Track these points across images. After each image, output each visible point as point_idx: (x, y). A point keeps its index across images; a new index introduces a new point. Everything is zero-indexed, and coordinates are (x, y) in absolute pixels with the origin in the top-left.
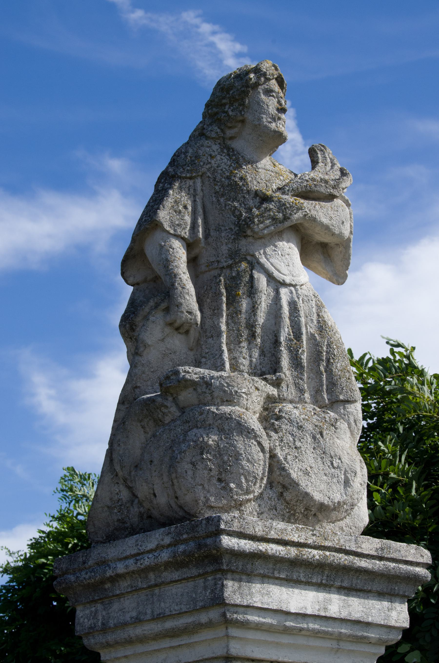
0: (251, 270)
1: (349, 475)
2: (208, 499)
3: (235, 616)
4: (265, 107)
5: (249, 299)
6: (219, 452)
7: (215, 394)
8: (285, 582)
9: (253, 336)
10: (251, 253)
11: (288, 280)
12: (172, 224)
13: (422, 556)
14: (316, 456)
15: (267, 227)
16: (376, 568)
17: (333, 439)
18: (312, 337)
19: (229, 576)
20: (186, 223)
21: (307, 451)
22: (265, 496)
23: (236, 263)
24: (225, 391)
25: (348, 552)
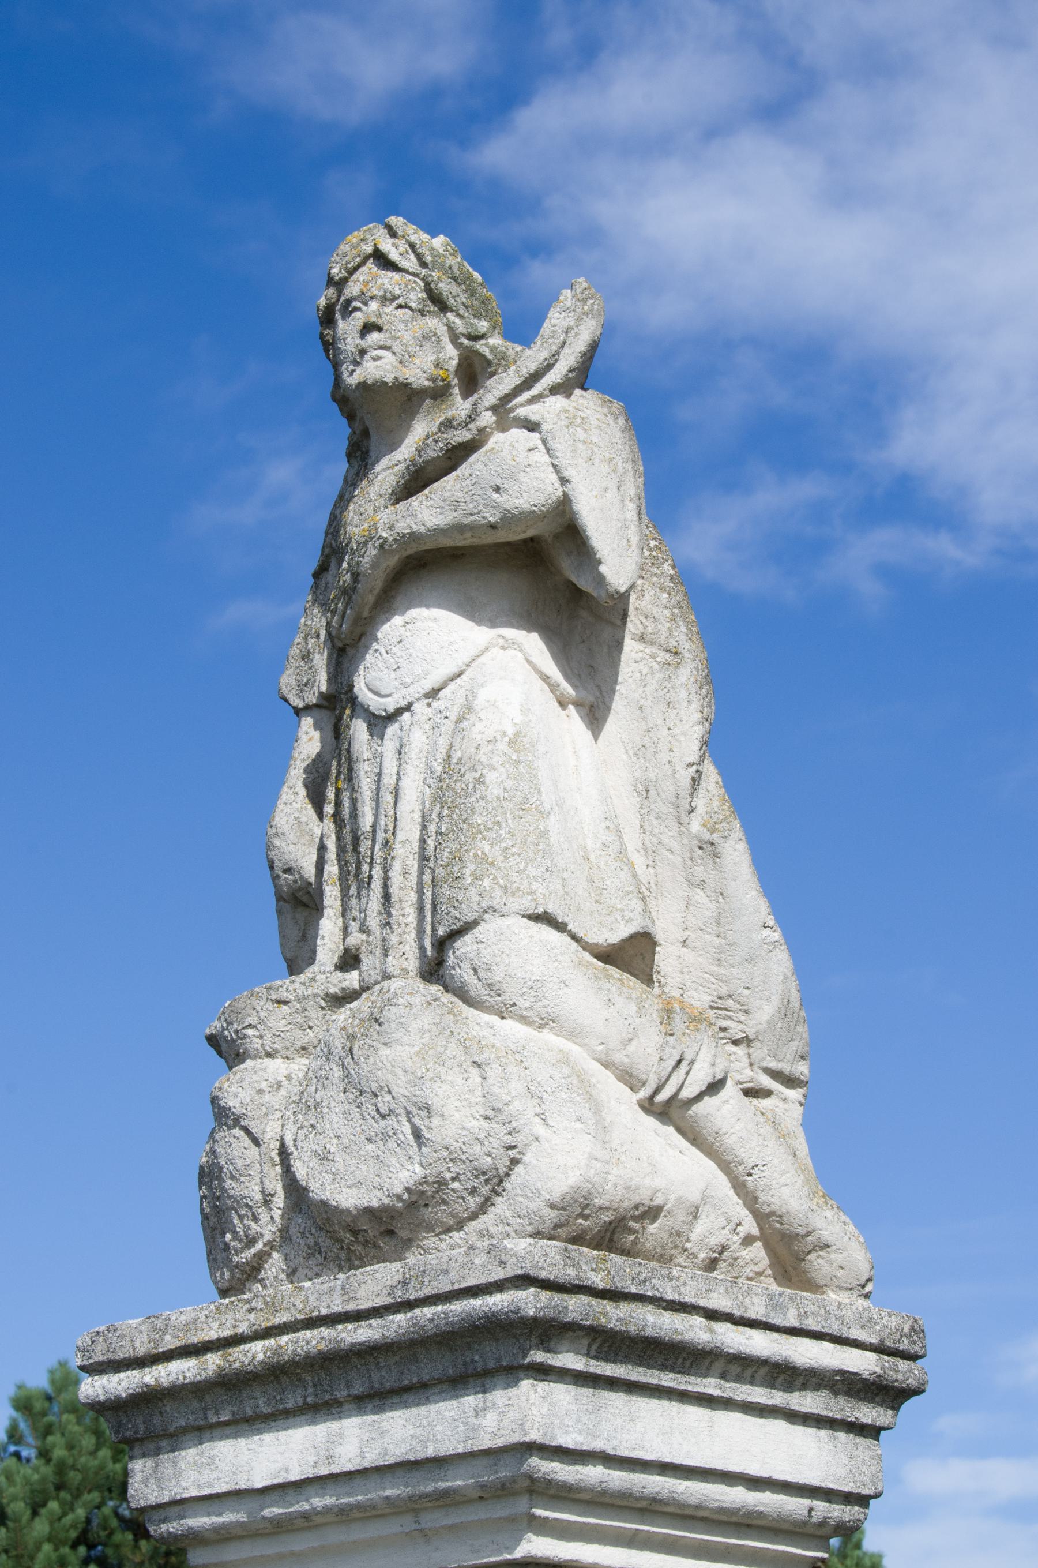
3: (164, 1527)
8: (245, 1426)
16: (391, 1334)
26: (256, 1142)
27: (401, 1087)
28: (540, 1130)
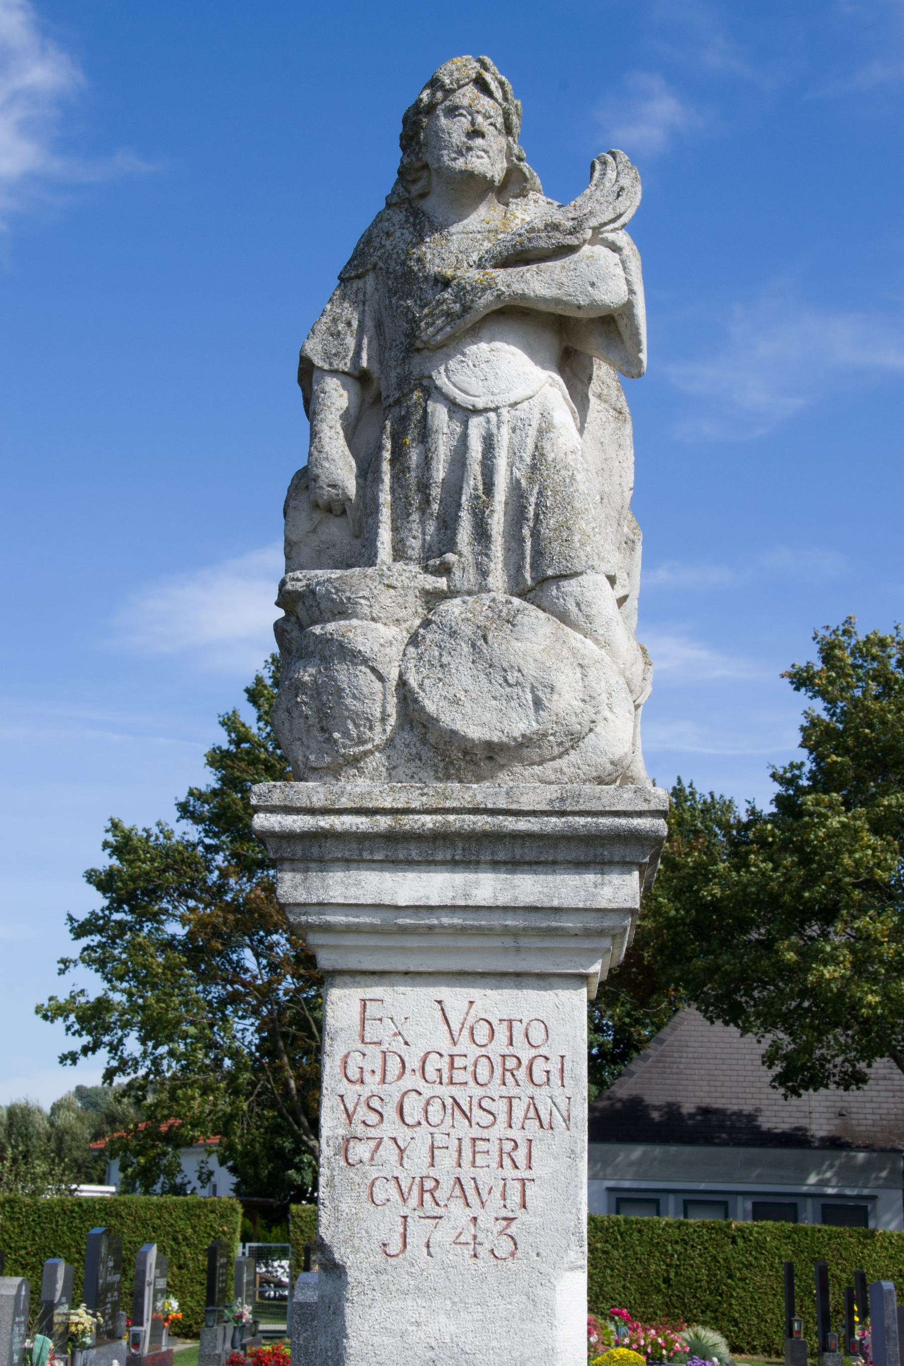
0: (426, 401)
1: (540, 694)
2: (308, 759)
3: (303, 918)
4: (446, 137)
5: (421, 446)
6: (317, 691)
7: (322, 606)
8: (391, 865)
9: (426, 501)
10: (426, 373)
11: (480, 403)
12: (328, 356)
13: (646, 800)
14: (475, 672)
15: (442, 329)
16: (548, 829)
17: (508, 642)
18: (515, 487)
19: (286, 866)
20: (347, 350)
21: (461, 668)
22: (398, 742)
23: (405, 395)
24: (333, 600)
25: (494, 812)
26: (381, 678)
27: (530, 670)
28: (607, 713)
